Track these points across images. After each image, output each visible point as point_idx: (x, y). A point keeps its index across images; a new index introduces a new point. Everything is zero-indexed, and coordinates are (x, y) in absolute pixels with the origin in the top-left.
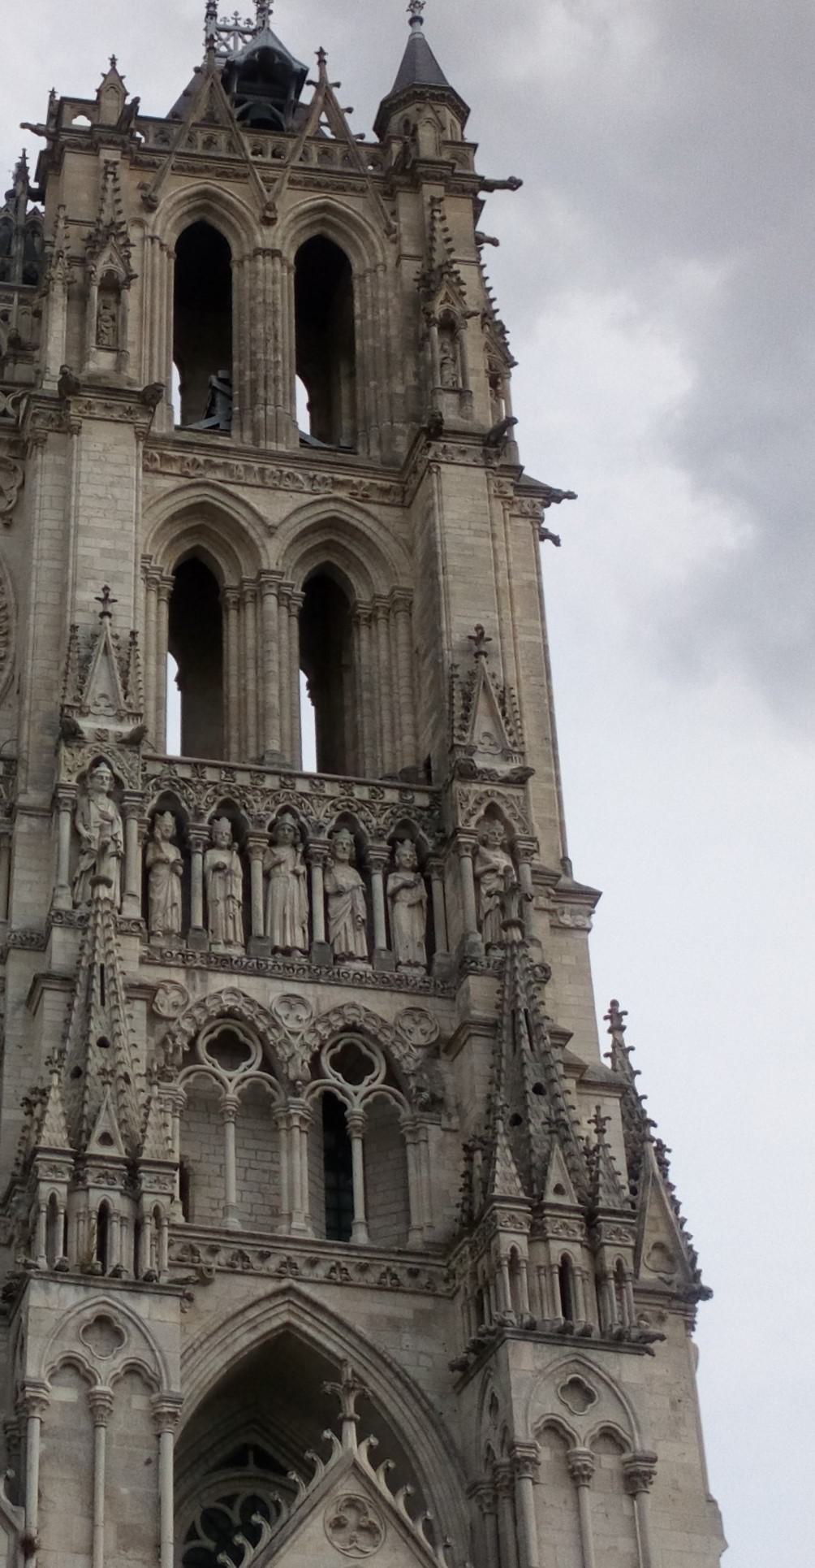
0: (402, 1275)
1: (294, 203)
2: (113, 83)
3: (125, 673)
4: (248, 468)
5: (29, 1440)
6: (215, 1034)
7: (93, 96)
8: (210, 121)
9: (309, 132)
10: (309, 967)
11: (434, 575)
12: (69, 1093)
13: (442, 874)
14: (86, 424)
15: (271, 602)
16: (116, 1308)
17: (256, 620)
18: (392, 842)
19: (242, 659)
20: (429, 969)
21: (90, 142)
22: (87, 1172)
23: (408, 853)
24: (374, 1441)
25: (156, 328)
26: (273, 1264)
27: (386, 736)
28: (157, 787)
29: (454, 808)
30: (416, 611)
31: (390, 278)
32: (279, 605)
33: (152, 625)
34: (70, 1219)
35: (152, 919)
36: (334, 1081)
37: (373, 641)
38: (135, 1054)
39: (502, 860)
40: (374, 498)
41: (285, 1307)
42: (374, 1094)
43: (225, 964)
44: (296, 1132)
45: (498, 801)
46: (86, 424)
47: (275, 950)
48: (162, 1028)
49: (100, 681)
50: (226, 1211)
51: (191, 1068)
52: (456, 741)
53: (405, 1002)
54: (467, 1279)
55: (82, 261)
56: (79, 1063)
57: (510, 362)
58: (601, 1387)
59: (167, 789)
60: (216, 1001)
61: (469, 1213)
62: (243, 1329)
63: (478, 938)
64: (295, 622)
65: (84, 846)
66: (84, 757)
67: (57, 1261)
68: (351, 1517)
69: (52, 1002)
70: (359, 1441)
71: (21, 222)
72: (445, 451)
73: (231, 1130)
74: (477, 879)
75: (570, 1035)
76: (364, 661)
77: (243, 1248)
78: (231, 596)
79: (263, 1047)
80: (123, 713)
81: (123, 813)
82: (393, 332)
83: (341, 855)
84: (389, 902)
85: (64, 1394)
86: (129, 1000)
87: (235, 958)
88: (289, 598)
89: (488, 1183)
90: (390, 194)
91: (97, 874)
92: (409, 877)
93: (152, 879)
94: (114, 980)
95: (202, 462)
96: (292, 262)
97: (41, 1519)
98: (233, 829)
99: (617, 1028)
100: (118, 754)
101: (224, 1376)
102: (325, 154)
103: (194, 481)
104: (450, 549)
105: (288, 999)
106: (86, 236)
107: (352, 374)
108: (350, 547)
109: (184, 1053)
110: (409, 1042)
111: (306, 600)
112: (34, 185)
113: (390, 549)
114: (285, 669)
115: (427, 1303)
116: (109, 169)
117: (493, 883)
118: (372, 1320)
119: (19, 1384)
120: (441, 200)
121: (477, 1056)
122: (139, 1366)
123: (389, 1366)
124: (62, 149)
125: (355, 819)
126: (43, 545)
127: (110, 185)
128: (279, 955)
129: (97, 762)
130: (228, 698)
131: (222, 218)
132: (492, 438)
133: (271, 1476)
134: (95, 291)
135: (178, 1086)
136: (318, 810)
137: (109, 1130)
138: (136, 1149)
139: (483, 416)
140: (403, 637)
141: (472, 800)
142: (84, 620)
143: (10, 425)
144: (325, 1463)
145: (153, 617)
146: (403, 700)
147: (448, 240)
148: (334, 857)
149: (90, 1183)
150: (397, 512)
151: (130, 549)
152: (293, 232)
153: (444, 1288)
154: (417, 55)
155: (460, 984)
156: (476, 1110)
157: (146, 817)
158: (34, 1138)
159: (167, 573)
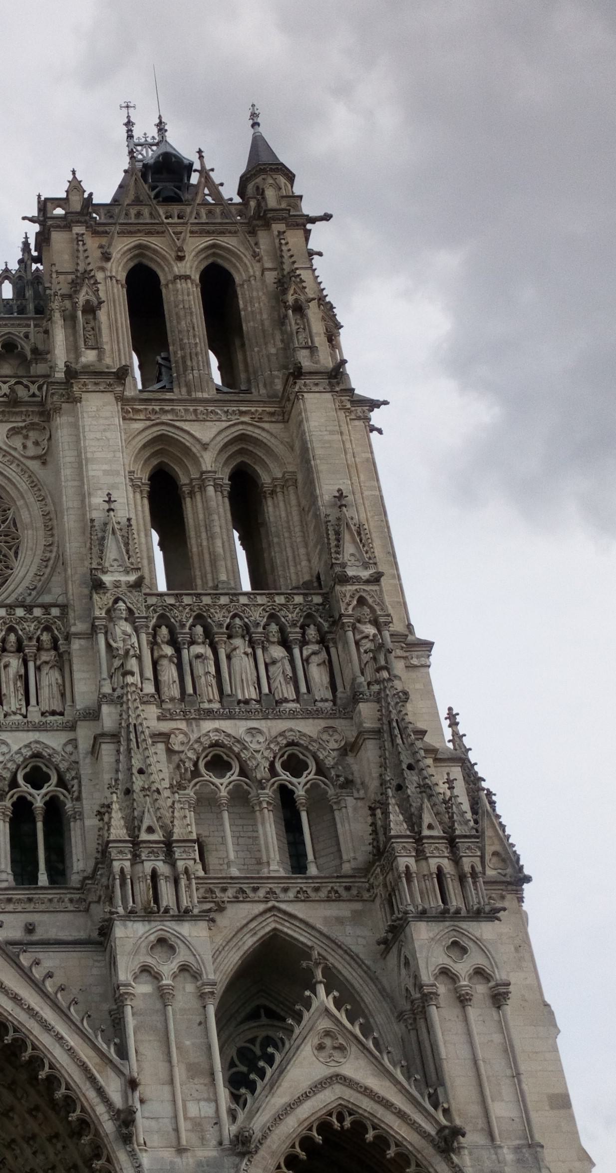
0: (341, 891)
1: (194, 245)
2: (75, 186)
3: (127, 544)
4: (186, 410)
5: (126, 1019)
6: (209, 758)
7: (64, 195)
8: (137, 201)
9: (198, 201)
11: (308, 461)
12: (124, 805)
13: (335, 643)
14: (84, 396)
15: (211, 490)
16: (169, 932)
17: (203, 502)
18: (302, 627)
19: (197, 527)
21: (66, 223)
22: (141, 851)
23: (313, 632)
24: (336, 994)
25: (120, 331)
26: (261, 893)
27: (291, 563)
28: (155, 611)
29: (338, 602)
30: (300, 485)
31: (259, 284)
32: (216, 491)
33: (140, 513)
34: (134, 882)
35: (162, 692)
36: (285, 777)
37: (276, 506)
38: (161, 776)
39: (371, 630)
40: (266, 419)
41: (272, 919)
42: (310, 782)
43: (210, 714)
44: (266, 811)
45: (364, 594)
46: (84, 396)
47: (239, 702)
48: (176, 758)
49: (112, 551)
50: (229, 865)
51: (196, 780)
52: (334, 561)
53: (322, 723)
54: (381, 888)
55: (70, 297)
56: (128, 785)
57: (339, 326)
58: (471, 944)
59: (161, 612)
60: (207, 738)
61: (377, 848)
62: (248, 936)
63: (362, 679)
64: (226, 500)
65: (115, 653)
66: (108, 599)
67: (130, 908)
68: (328, 1042)
69: (107, 750)
70: (327, 995)
71: (30, 277)
72: (305, 385)
73: (226, 815)
74: (357, 643)
75: (426, 732)
76: (272, 519)
77: (242, 886)
78: (186, 489)
79: (239, 762)
80: (128, 569)
81: (136, 630)
82: (265, 316)
83: (272, 639)
84: (305, 664)
85: (143, 988)
86: (154, 743)
87: (215, 710)
88: (221, 486)
89: (386, 828)
90: (253, 232)
91: (125, 669)
92: (316, 647)
93: (159, 668)
94: (143, 732)
95: (158, 410)
96: (198, 281)
97: (139, 1066)
98: (204, 632)
99: (454, 724)
100: (129, 594)
101: (240, 965)
102: (210, 213)
103: (154, 422)
104: (316, 445)
105: (251, 731)
106: (70, 281)
107: (243, 345)
108: (254, 451)
109: (192, 771)
111: (232, 487)
112: (35, 254)
113: (279, 449)
114: (224, 530)
115: (358, 906)
116: (79, 238)
117: (367, 645)
118: (326, 920)
119: (115, 986)
120: (284, 232)
121: (370, 752)
122: (188, 966)
123: (340, 947)
124: (49, 230)
126: (67, 473)
127: (81, 248)
128: (242, 705)
129: (116, 601)
131: (152, 259)
132: (333, 374)
133: (276, 1023)
134: (80, 313)
135: (190, 792)
136: (255, 613)
137: (151, 824)
138: (169, 834)
139: (326, 361)
140: (294, 502)
141: (348, 596)
142: (98, 515)
143: (37, 402)
144: (308, 1011)
145: (140, 508)
146: (299, 540)
147: (292, 256)
148: (268, 641)
149: (144, 858)
150: (281, 426)
151: (121, 468)
152: (196, 263)
153: (368, 895)
154: (259, 146)
155: (354, 709)
156: (374, 784)
157: (150, 630)
158: (106, 835)
159: (145, 480)
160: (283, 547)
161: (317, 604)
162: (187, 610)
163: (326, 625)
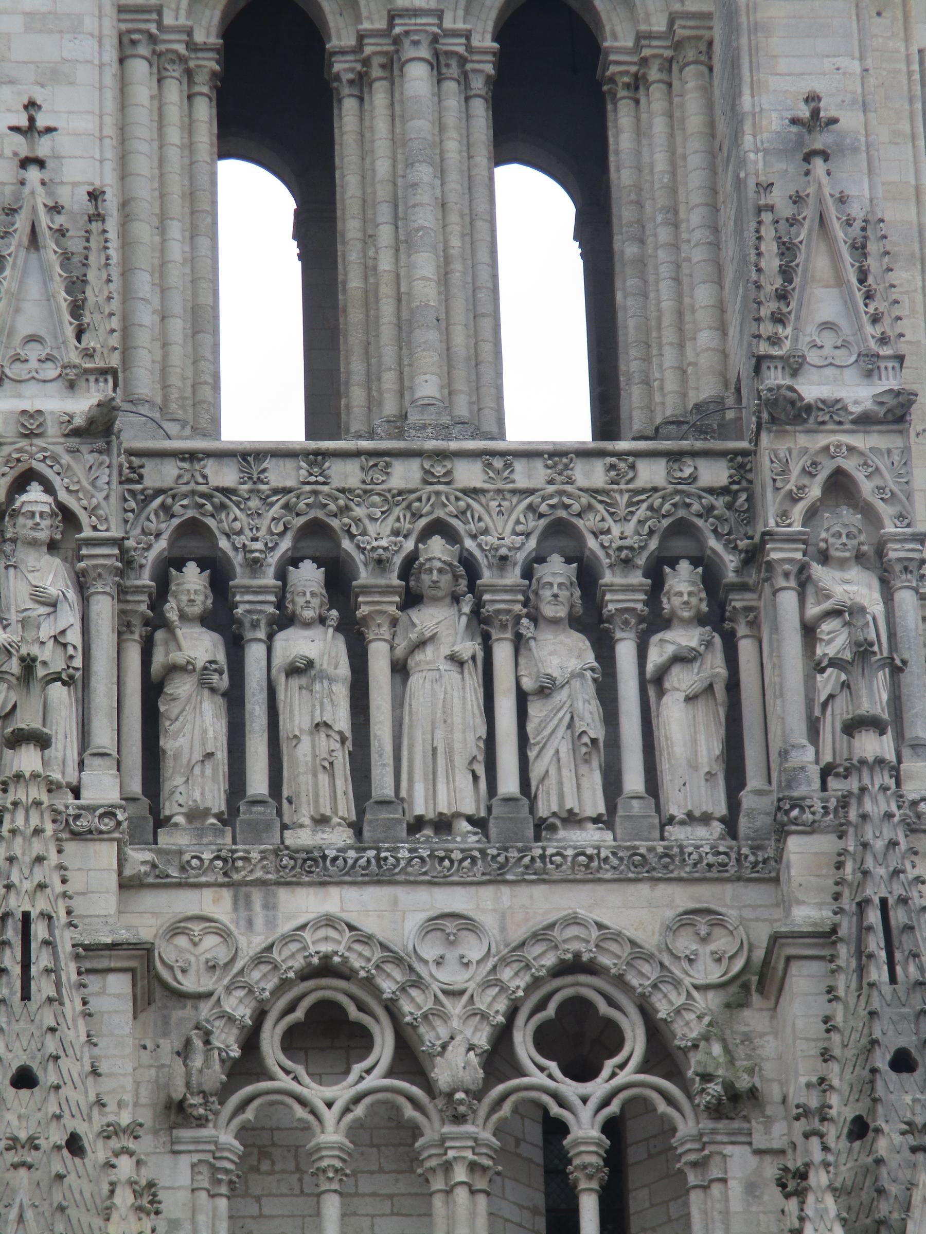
6: (299, 1014)
10: (483, 852)
13: (754, 624)
20: (730, 823)
23: (684, 587)
35: (166, 787)
36: (539, 1078)
44: (462, 1194)
45: (850, 465)
47: (417, 825)
48: (183, 1014)
51: (248, 1090)
52: (763, 348)
59: (190, 513)
60: (294, 947)
64: (480, 109)
73: (332, 1207)
83: (549, 611)
84: (652, 693)
87: (331, 853)
100: (66, 459)
110: (687, 981)
125: (574, 527)
129: (21, 484)
130: (345, 290)
136: (500, 521)
140: (694, 120)
141: (796, 470)
145: (174, 135)
157: (146, 579)
160: (651, 278)
161: (711, 491)
162: (275, 511)
163: (731, 561)
